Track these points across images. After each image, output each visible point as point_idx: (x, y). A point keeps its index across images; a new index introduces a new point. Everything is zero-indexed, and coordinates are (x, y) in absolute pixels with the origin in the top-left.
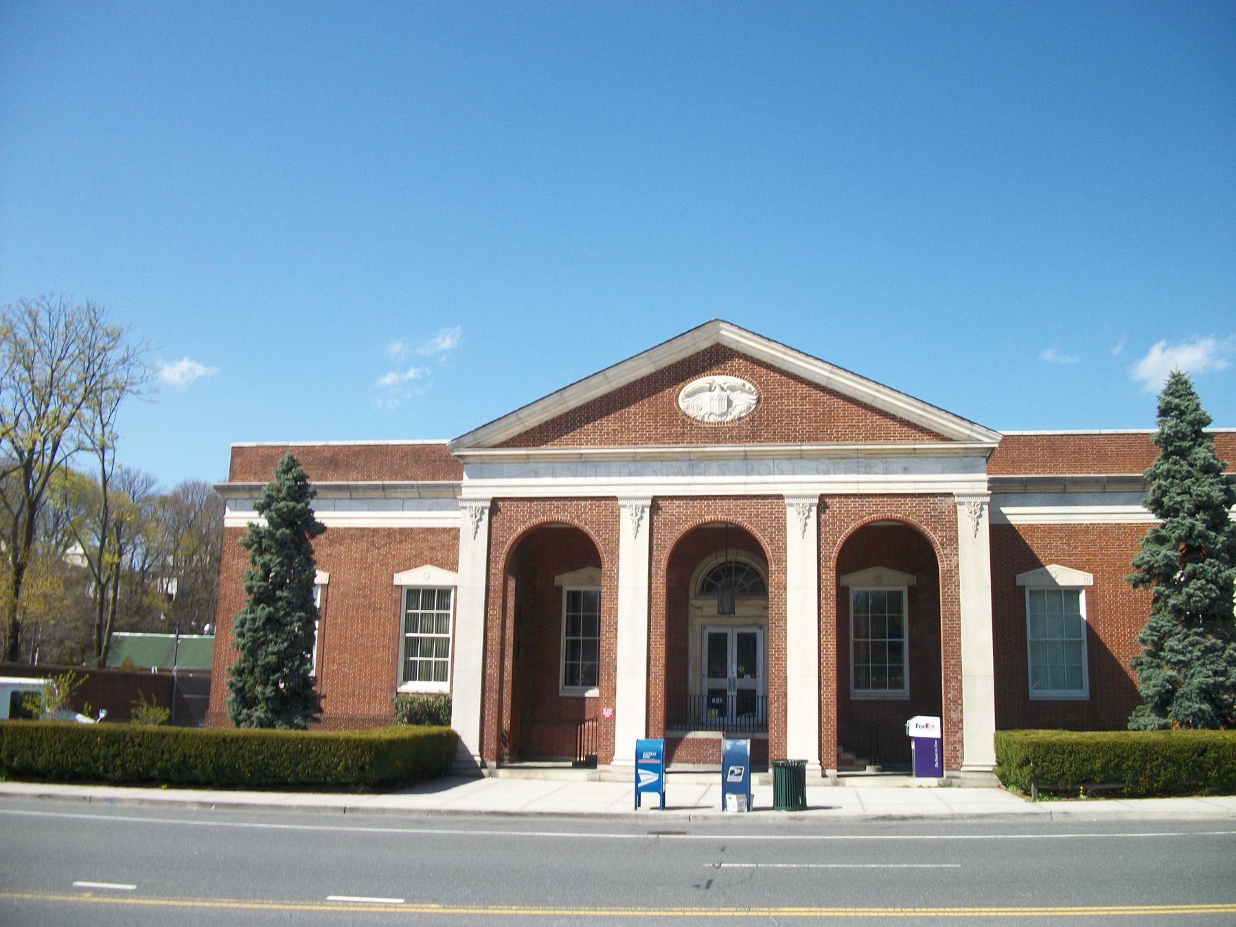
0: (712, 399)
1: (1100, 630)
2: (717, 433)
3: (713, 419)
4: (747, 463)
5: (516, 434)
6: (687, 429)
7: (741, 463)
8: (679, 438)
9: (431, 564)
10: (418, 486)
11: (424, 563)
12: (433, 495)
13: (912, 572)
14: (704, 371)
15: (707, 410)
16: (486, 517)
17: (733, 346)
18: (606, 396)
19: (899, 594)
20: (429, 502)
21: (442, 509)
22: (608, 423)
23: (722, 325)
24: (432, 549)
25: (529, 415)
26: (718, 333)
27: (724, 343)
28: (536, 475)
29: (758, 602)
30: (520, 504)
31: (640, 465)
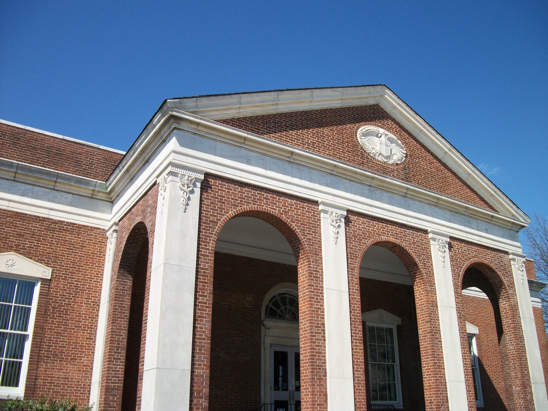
0: (378, 142)
1: (484, 362)
2: (384, 169)
3: (380, 158)
4: (406, 199)
5: (248, 115)
6: (363, 158)
7: (402, 199)
8: (361, 164)
9: (17, 251)
10: (18, 167)
11: (9, 249)
12: (30, 180)
13: (399, 316)
14: (371, 121)
15: (378, 148)
16: (198, 191)
17: (388, 110)
18: (305, 113)
19: (391, 330)
20: (23, 187)
21: (36, 197)
22: (309, 134)
23: (387, 91)
24: (20, 235)
25: (248, 103)
26: (382, 96)
27: (382, 106)
28: (248, 162)
29: (294, 325)
30: (232, 186)
31: (334, 178)
